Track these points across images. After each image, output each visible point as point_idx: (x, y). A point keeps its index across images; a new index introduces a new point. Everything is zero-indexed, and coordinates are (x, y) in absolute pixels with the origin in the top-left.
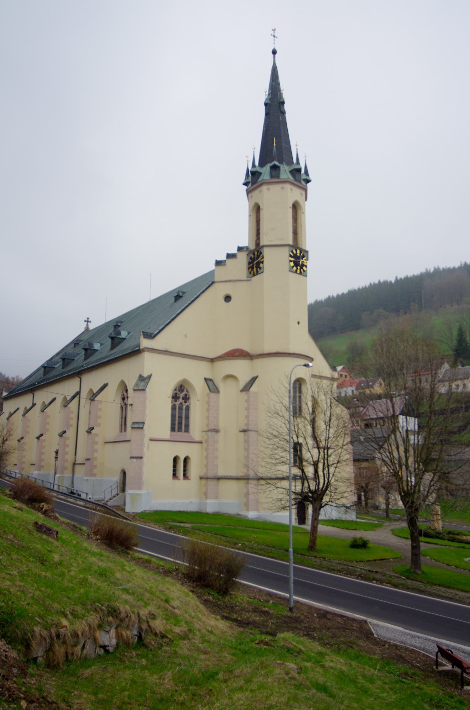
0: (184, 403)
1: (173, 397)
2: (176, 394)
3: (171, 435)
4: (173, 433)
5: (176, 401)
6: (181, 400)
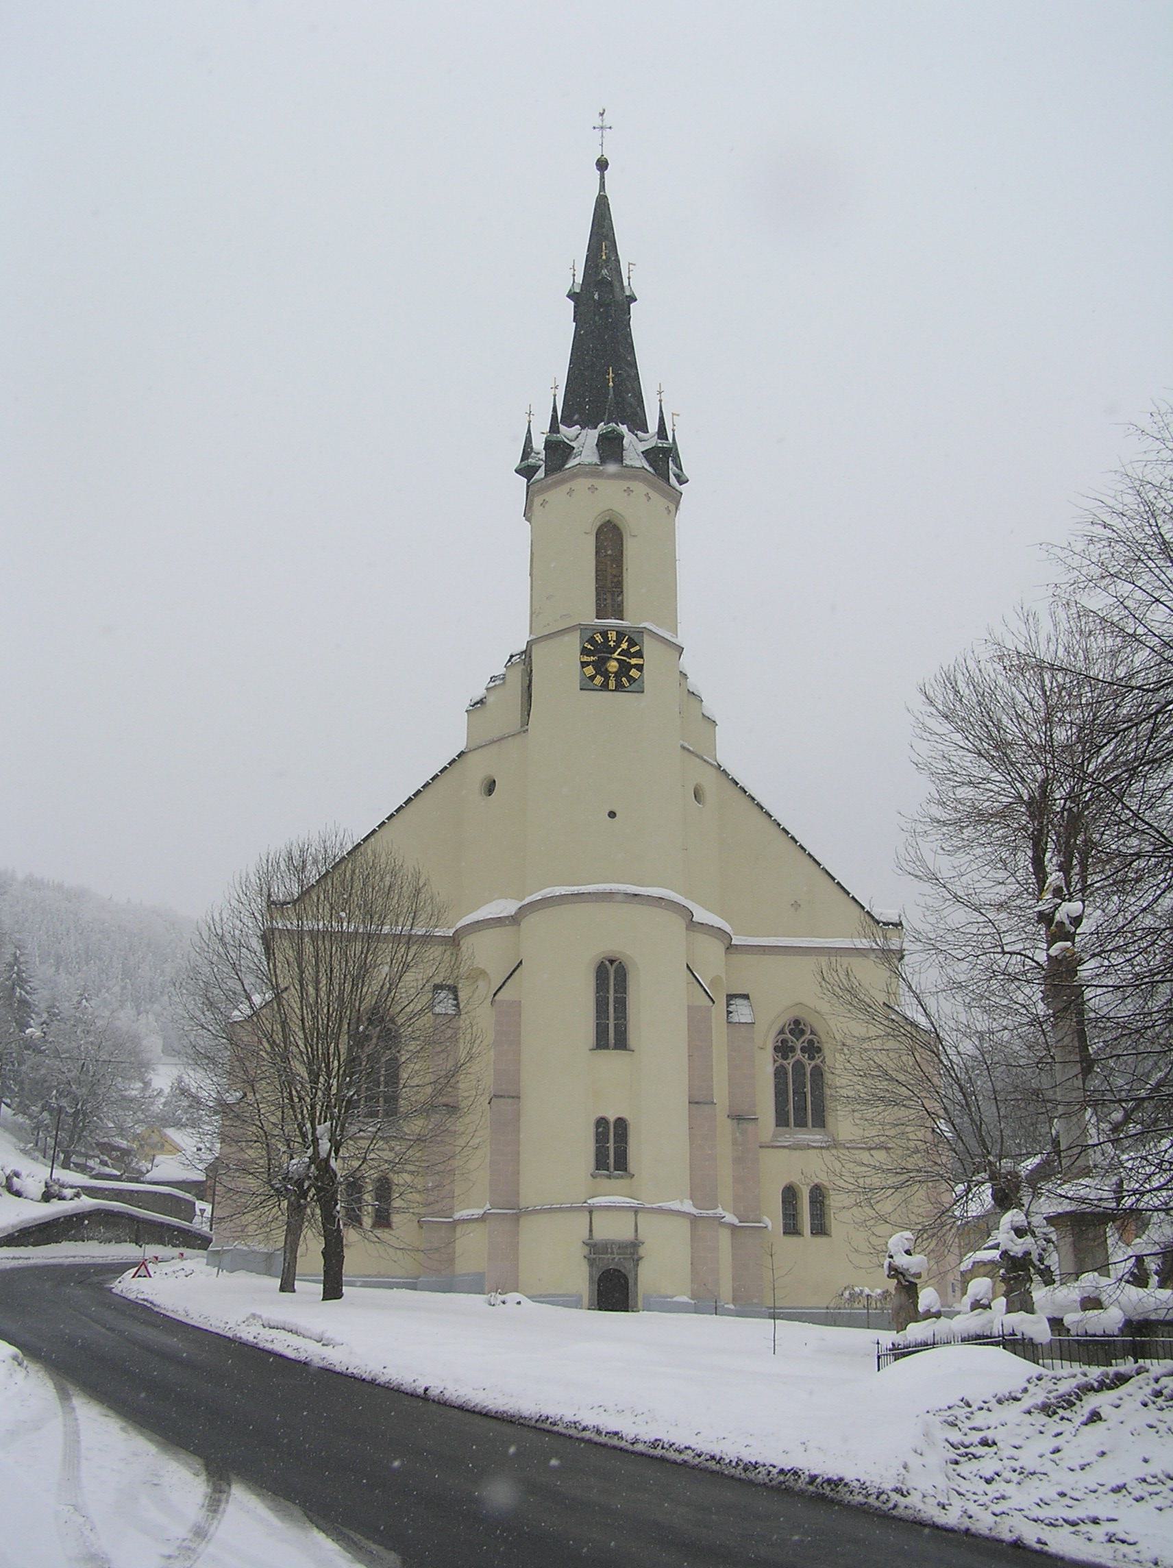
1: (776, 1049)
3: (775, 1135)
5: (785, 1057)
6: (799, 1054)
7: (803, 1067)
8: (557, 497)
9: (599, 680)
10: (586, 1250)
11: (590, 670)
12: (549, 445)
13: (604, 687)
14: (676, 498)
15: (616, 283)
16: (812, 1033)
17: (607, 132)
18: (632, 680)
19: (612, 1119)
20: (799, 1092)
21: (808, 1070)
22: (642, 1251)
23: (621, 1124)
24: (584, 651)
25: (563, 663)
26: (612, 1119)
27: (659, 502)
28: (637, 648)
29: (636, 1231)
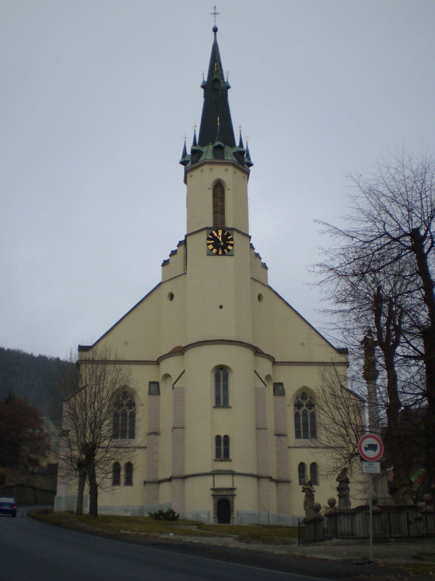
0: (308, 410)
1: (295, 406)
2: (299, 402)
4: (298, 440)
5: (299, 409)
6: (305, 407)
7: (307, 412)
8: (196, 173)
9: (215, 251)
10: (212, 492)
11: (211, 247)
12: (193, 151)
13: (217, 254)
14: (247, 173)
15: (221, 81)
16: (311, 398)
17: (217, 16)
18: (229, 250)
19: (222, 435)
20: (305, 424)
21: (309, 414)
22: (235, 492)
23: (227, 438)
24: (209, 239)
25: (201, 243)
26: (222, 435)
27: (240, 174)
28: (231, 237)
29: (233, 484)
